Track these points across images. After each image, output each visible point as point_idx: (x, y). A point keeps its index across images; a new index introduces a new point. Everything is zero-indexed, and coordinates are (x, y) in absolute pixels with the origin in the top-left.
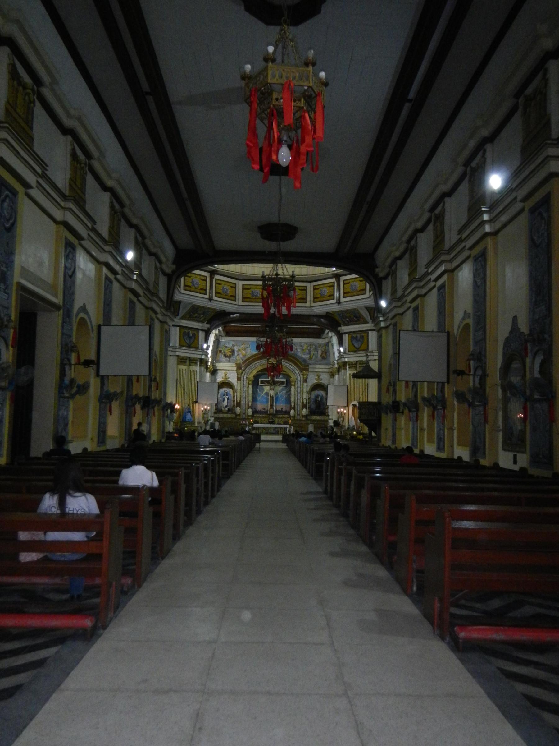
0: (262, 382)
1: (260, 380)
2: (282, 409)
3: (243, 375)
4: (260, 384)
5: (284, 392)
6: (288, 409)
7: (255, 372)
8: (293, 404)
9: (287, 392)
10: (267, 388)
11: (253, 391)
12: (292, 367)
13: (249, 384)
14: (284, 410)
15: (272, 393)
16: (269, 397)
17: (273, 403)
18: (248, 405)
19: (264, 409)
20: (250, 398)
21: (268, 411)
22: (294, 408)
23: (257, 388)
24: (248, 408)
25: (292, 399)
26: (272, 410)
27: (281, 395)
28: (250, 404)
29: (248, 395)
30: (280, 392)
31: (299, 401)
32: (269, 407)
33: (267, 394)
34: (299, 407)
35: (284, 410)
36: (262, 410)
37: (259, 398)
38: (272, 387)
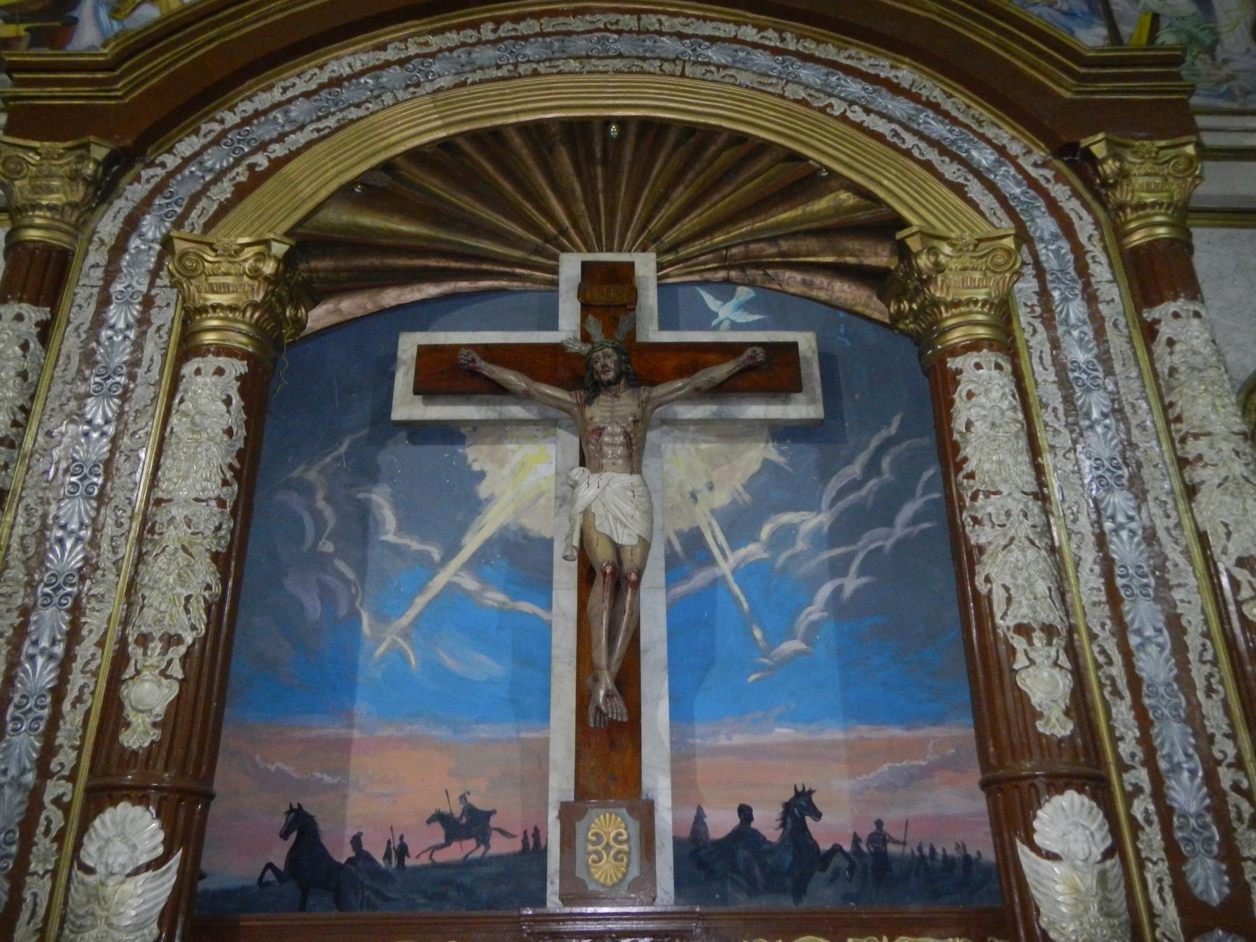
0: (444, 374)
1: (409, 344)
2: (800, 807)
3: (108, 226)
4: (407, 406)
5: (811, 522)
6: (950, 810)
7: (314, 180)
8: (1043, 683)
9: (845, 529)
10: (524, 476)
11: (249, 471)
12: (900, 107)
13: (188, 347)
14: (833, 827)
15: (613, 504)
16: (565, 596)
17: (628, 681)
18: (113, 713)
19: (472, 824)
20: (178, 594)
21: (534, 851)
22: (1086, 768)
23: (368, 473)
24: (101, 796)
25: (1013, 580)
26: (608, 825)
27: (745, 573)
28: (151, 695)
29: (148, 528)
30: (739, 524)
31: (1144, 615)
32: (561, 782)
33: (521, 558)
34: (1173, 738)
35: (833, 827)
36: (425, 847)
37: (385, 639)
38: (612, 411)
